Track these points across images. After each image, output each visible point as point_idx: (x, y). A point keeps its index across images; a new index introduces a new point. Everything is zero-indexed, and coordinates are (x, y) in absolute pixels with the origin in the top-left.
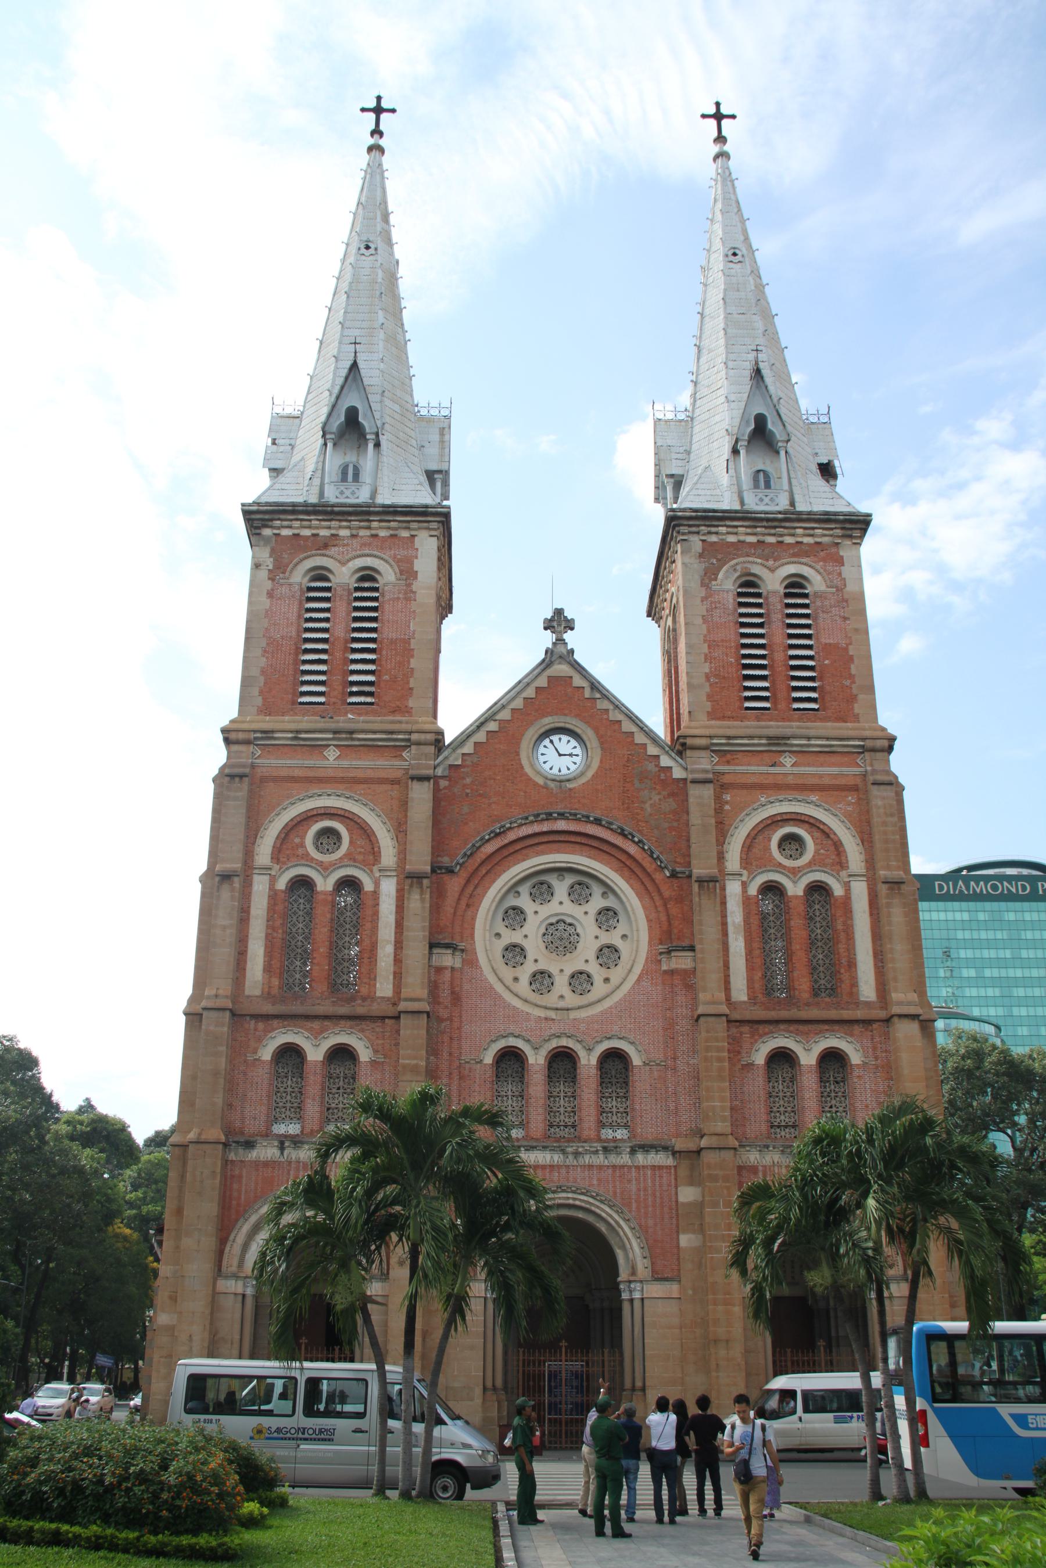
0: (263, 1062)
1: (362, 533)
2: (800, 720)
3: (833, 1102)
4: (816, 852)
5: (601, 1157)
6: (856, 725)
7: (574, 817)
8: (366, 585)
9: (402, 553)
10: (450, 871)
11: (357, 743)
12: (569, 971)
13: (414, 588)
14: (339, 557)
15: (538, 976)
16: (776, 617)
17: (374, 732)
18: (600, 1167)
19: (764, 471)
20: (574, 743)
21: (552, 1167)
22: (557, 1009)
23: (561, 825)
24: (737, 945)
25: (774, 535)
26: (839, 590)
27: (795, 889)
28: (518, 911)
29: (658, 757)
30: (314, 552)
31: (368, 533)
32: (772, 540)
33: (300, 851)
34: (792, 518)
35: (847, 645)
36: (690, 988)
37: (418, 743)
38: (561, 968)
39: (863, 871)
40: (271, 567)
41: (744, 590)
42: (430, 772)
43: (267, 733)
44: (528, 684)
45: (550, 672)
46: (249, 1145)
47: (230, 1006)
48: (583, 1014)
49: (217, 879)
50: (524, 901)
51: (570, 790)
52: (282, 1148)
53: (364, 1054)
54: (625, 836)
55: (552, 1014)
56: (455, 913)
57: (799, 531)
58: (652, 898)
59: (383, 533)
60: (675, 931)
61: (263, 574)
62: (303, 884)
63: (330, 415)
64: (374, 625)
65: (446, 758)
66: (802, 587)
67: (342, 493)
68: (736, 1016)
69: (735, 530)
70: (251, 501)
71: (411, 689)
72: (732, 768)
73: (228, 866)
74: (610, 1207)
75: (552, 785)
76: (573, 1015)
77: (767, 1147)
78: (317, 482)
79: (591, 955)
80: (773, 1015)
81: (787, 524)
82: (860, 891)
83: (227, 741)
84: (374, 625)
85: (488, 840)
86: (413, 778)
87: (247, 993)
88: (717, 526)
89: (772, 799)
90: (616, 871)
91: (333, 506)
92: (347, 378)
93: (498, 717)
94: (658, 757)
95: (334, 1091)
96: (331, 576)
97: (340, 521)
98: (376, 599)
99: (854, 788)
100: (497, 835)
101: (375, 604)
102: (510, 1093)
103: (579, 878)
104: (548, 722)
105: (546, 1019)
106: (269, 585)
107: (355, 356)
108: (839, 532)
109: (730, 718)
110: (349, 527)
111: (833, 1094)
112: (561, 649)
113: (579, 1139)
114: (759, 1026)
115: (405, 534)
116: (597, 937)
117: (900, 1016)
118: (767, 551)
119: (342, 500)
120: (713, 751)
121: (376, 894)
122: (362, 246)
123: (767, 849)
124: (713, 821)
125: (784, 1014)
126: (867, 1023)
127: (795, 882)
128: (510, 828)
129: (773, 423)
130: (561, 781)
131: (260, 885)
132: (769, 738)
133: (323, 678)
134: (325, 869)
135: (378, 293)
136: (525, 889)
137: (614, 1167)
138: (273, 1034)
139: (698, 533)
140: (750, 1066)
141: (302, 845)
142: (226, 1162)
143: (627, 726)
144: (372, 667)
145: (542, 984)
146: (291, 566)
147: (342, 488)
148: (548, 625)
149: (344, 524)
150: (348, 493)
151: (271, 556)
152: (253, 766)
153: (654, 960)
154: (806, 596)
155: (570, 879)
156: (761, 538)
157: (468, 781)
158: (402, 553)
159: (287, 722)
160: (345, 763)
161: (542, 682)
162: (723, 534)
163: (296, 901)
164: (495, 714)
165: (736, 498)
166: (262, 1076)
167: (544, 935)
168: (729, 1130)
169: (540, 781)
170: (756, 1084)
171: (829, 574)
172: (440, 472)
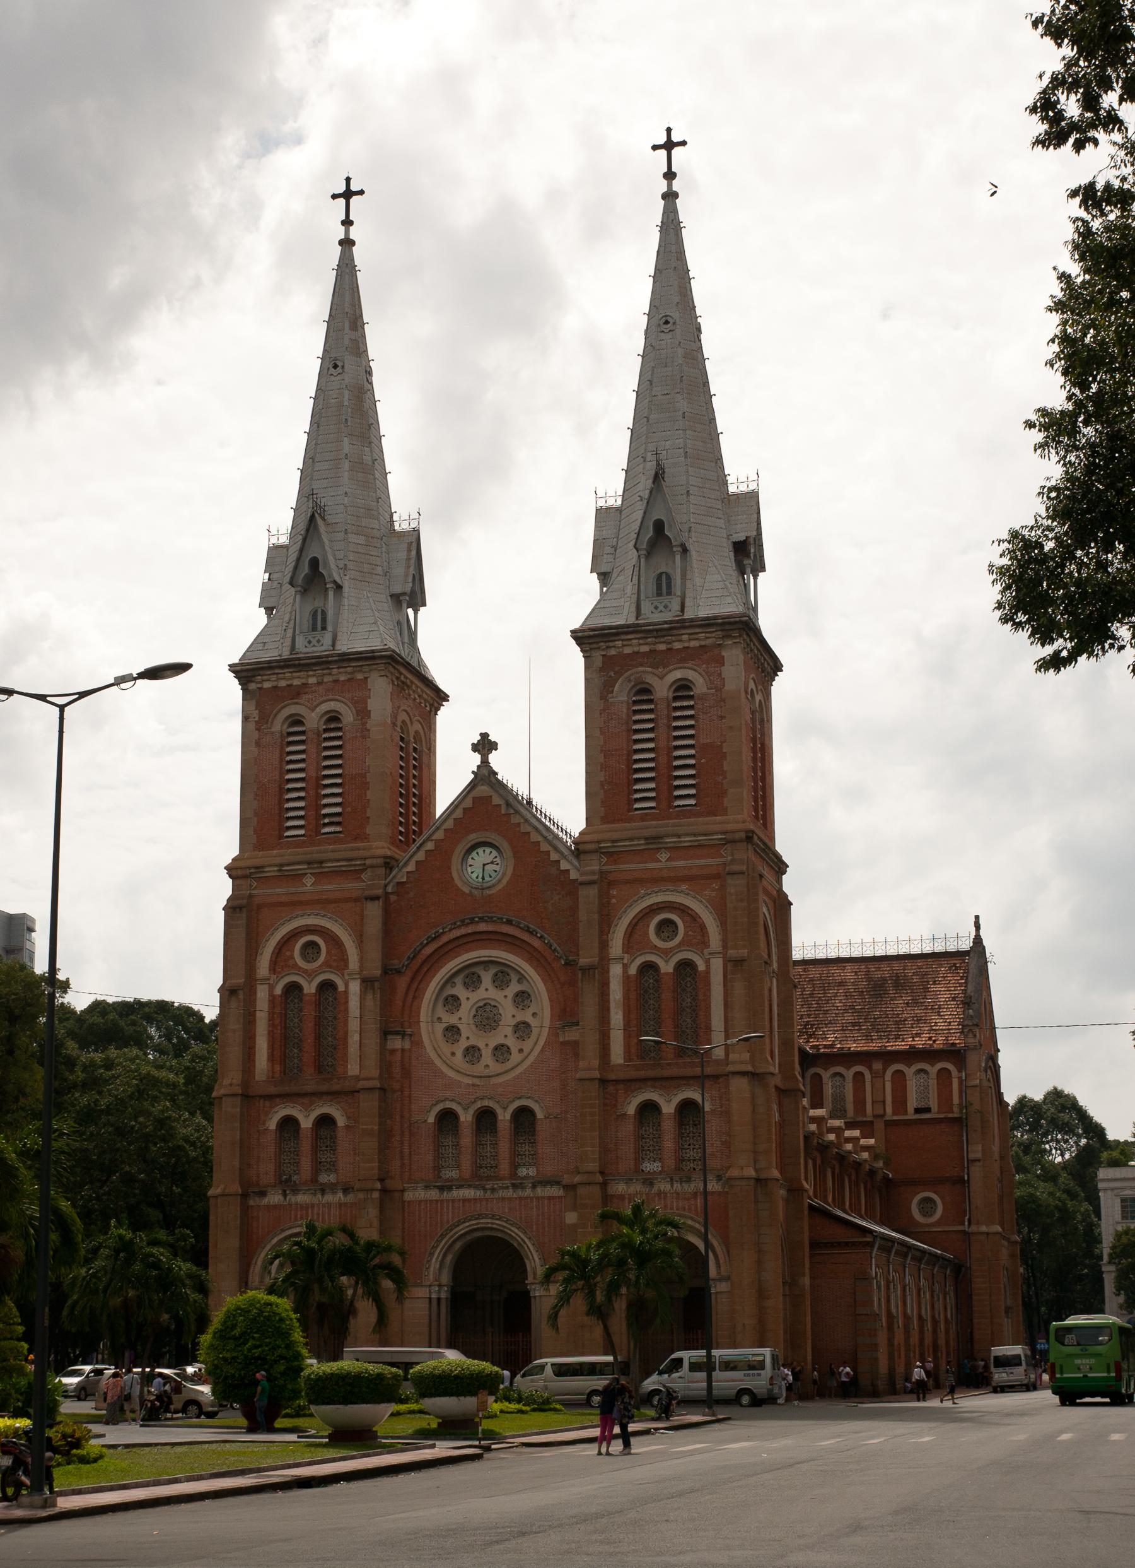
0: (271, 1130)
2: (678, 817)
3: (691, 1141)
4: (686, 934)
5: (511, 1190)
6: (724, 817)
7: (490, 920)
10: (398, 972)
11: (326, 870)
12: (492, 1045)
15: (471, 1050)
16: (663, 722)
17: (338, 861)
18: (510, 1199)
20: (495, 853)
21: (475, 1200)
22: (481, 1077)
23: (482, 927)
24: (617, 1017)
25: (664, 642)
26: (719, 690)
27: (667, 967)
28: (455, 998)
29: (558, 862)
31: (330, 678)
33: (291, 962)
34: (681, 625)
35: (722, 743)
36: (576, 1055)
37: (372, 867)
38: (487, 1043)
39: (720, 949)
40: (257, 719)
41: (639, 698)
42: (380, 892)
43: (259, 868)
44: (457, 806)
45: (475, 793)
46: (263, 1194)
47: (240, 1092)
48: (501, 1079)
49: (227, 993)
50: (459, 991)
51: (490, 895)
52: (285, 1195)
53: (341, 1121)
54: (531, 933)
55: (477, 1081)
56: (404, 1005)
57: (685, 637)
58: (553, 982)
60: (568, 1009)
61: (252, 726)
62: (293, 989)
63: (296, 568)
64: (339, 762)
65: (394, 877)
66: (690, 689)
67: (310, 642)
68: (612, 1076)
69: (630, 643)
70: (237, 661)
71: (368, 818)
72: (618, 866)
73: (235, 981)
74: (518, 1229)
75: (475, 892)
76: (494, 1081)
77: (632, 1180)
78: (290, 633)
79: (509, 1031)
80: (642, 1074)
81: (675, 632)
82: (717, 964)
83: (230, 876)
84: (339, 762)
85: (427, 944)
86: (366, 899)
87: (257, 1078)
88: (615, 641)
89: (649, 891)
90: (526, 961)
91: (299, 659)
92: (308, 530)
93: (433, 838)
94: (558, 862)
95: (324, 1148)
97: (307, 671)
98: (339, 738)
99: (717, 876)
100: (434, 939)
101: (339, 743)
102: (450, 1143)
103: (501, 968)
104: (473, 838)
105: (473, 1085)
106: (256, 735)
109: (622, 821)
110: (314, 676)
111: (691, 1135)
112: (485, 772)
113: (498, 1178)
114: (632, 1084)
115: (360, 676)
116: (514, 1016)
117: (734, 1073)
120: (603, 853)
121: (346, 992)
122: (331, 366)
123: (646, 934)
124: (596, 916)
125: (650, 1073)
126: (716, 1077)
127: (667, 962)
128: (443, 933)
129: (670, 526)
130: (483, 889)
131: (262, 994)
132: (646, 839)
133: (302, 813)
134: (310, 975)
136: (459, 980)
137: (520, 1198)
138: (275, 1110)
139: (599, 648)
140: (625, 1115)
141: (292, 957)
142: (245, 1210)
143: (534, 837)
144: (339, 800)
145: (473, 1056)
148: (475, 748)
149: (311, 673)
152: (251, 896)
153: (554, 1032)
154: (691, 697)
155: (493, 970)
157: (412, 894)
159: (274, 857)
160: (319, 888)
161: (468, 803)
162: (618, 648)
163: (292, 1001)
164: (431, 835)
165: (633, 609)
166: (270, 1141)
167: (475, 1016)
168: (597, 1169)
169: (466, 890)
170: (627, 1130)
172: (404, 594)
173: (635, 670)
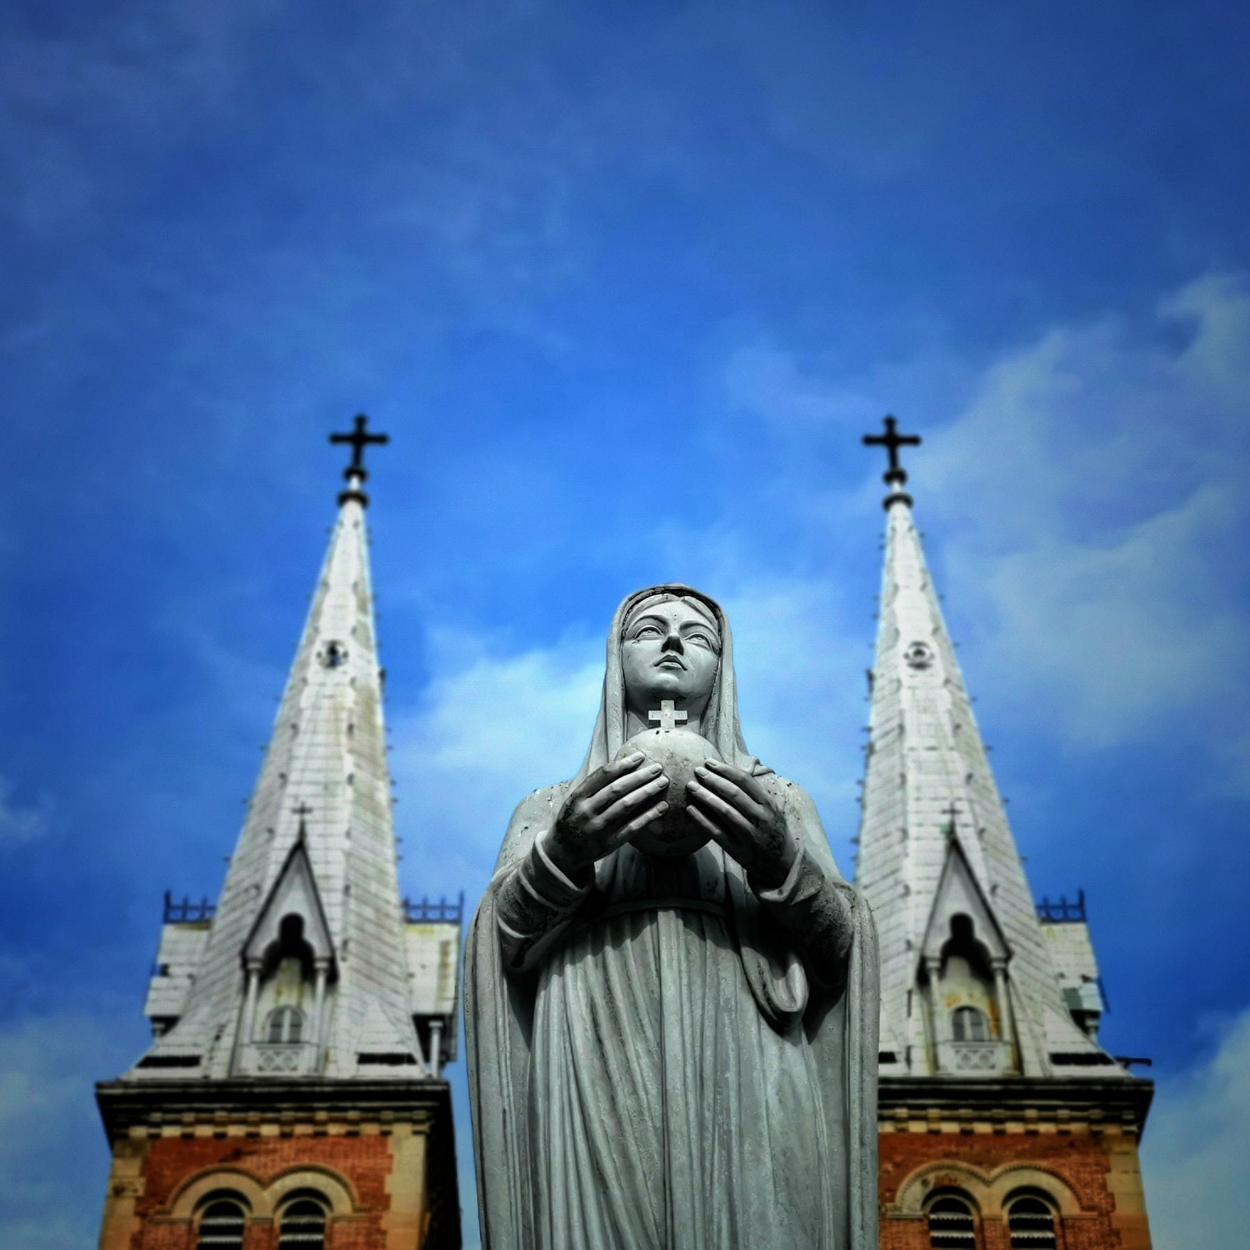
1: (300, 1129)
8: (303, 1220)
9: (364, 1163)
13: (384, 1224)
14: (261, 1173)
19: (971, 1009)
26: (1105, 1213)
30: (216, 1165)
32: (984, 1128)
40: (141, 1193)
57: (1031, 1113)
59: (333, 1129)
61: (127, 1205)
69: (922, 1113)
91: (252, 1085)
92: (286, 868)
96: (244, 1208)
106: (135, 1224)
107: (302, 834)
108: (1096, 1113)
115: (371, 1129)
118: (977, 1148)
119: (268, 1073)
135: (344, 726)
146: (175, 1190)
147: (270, 1052)
149: (270, 1115)
150: (279, 1061)
151: (142, 1173)
156: (967, 1126)
158: (364, 1163)
171: (1086, 1185)
173: (934, 1163)
